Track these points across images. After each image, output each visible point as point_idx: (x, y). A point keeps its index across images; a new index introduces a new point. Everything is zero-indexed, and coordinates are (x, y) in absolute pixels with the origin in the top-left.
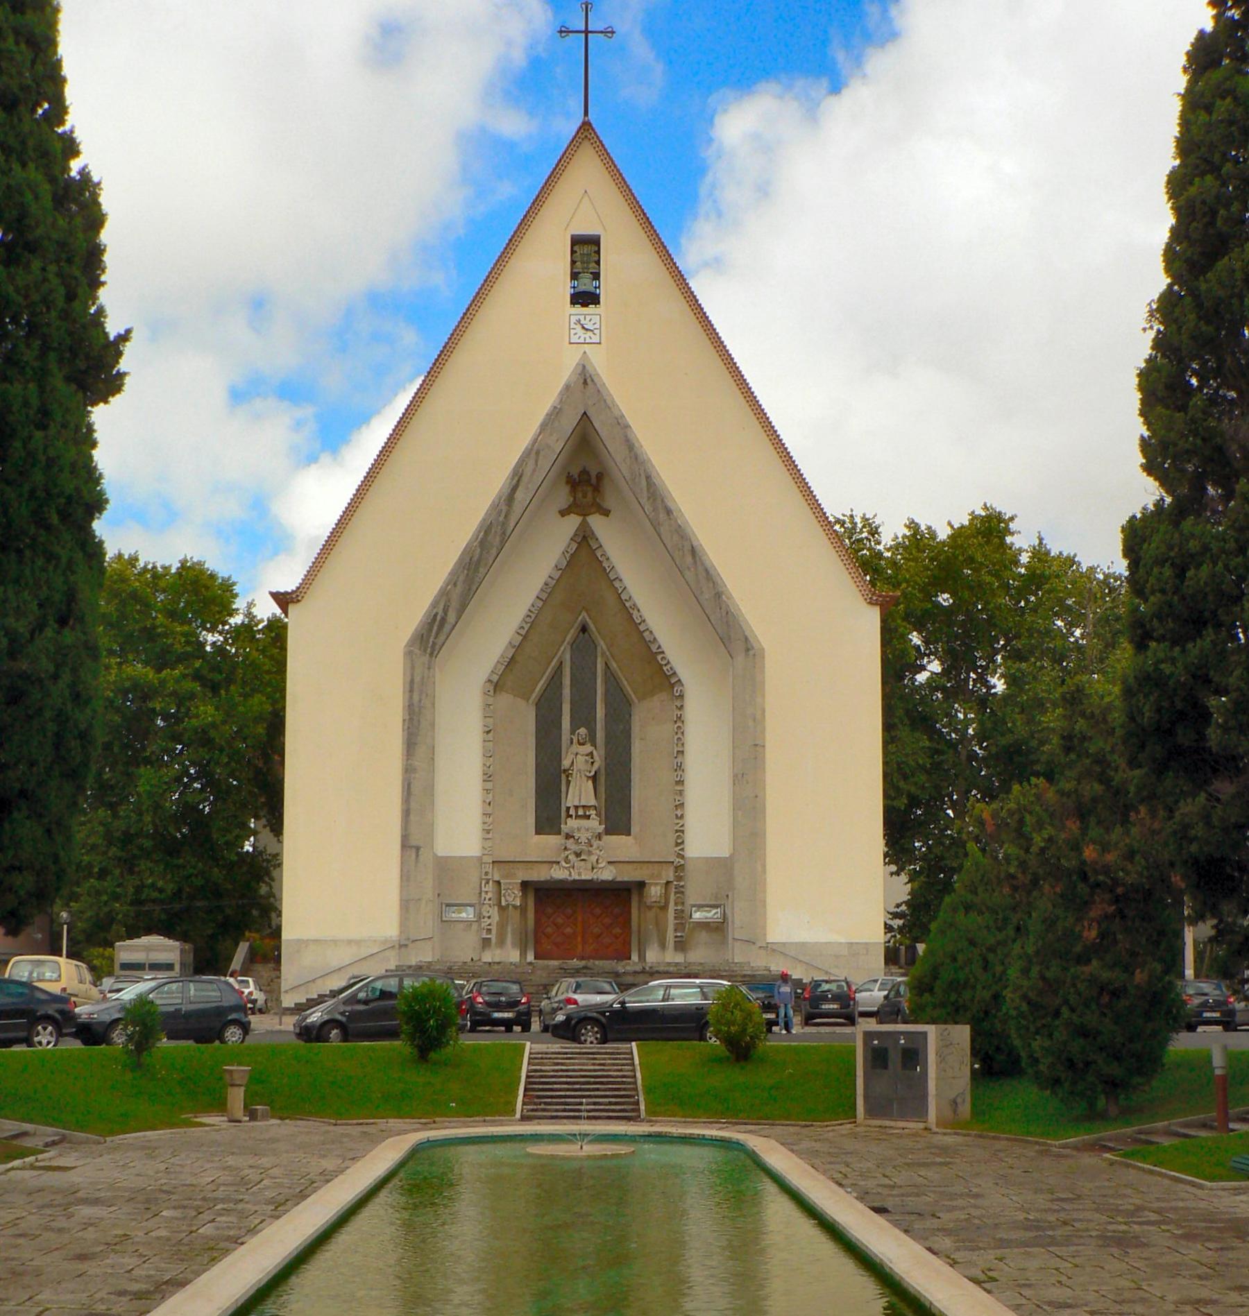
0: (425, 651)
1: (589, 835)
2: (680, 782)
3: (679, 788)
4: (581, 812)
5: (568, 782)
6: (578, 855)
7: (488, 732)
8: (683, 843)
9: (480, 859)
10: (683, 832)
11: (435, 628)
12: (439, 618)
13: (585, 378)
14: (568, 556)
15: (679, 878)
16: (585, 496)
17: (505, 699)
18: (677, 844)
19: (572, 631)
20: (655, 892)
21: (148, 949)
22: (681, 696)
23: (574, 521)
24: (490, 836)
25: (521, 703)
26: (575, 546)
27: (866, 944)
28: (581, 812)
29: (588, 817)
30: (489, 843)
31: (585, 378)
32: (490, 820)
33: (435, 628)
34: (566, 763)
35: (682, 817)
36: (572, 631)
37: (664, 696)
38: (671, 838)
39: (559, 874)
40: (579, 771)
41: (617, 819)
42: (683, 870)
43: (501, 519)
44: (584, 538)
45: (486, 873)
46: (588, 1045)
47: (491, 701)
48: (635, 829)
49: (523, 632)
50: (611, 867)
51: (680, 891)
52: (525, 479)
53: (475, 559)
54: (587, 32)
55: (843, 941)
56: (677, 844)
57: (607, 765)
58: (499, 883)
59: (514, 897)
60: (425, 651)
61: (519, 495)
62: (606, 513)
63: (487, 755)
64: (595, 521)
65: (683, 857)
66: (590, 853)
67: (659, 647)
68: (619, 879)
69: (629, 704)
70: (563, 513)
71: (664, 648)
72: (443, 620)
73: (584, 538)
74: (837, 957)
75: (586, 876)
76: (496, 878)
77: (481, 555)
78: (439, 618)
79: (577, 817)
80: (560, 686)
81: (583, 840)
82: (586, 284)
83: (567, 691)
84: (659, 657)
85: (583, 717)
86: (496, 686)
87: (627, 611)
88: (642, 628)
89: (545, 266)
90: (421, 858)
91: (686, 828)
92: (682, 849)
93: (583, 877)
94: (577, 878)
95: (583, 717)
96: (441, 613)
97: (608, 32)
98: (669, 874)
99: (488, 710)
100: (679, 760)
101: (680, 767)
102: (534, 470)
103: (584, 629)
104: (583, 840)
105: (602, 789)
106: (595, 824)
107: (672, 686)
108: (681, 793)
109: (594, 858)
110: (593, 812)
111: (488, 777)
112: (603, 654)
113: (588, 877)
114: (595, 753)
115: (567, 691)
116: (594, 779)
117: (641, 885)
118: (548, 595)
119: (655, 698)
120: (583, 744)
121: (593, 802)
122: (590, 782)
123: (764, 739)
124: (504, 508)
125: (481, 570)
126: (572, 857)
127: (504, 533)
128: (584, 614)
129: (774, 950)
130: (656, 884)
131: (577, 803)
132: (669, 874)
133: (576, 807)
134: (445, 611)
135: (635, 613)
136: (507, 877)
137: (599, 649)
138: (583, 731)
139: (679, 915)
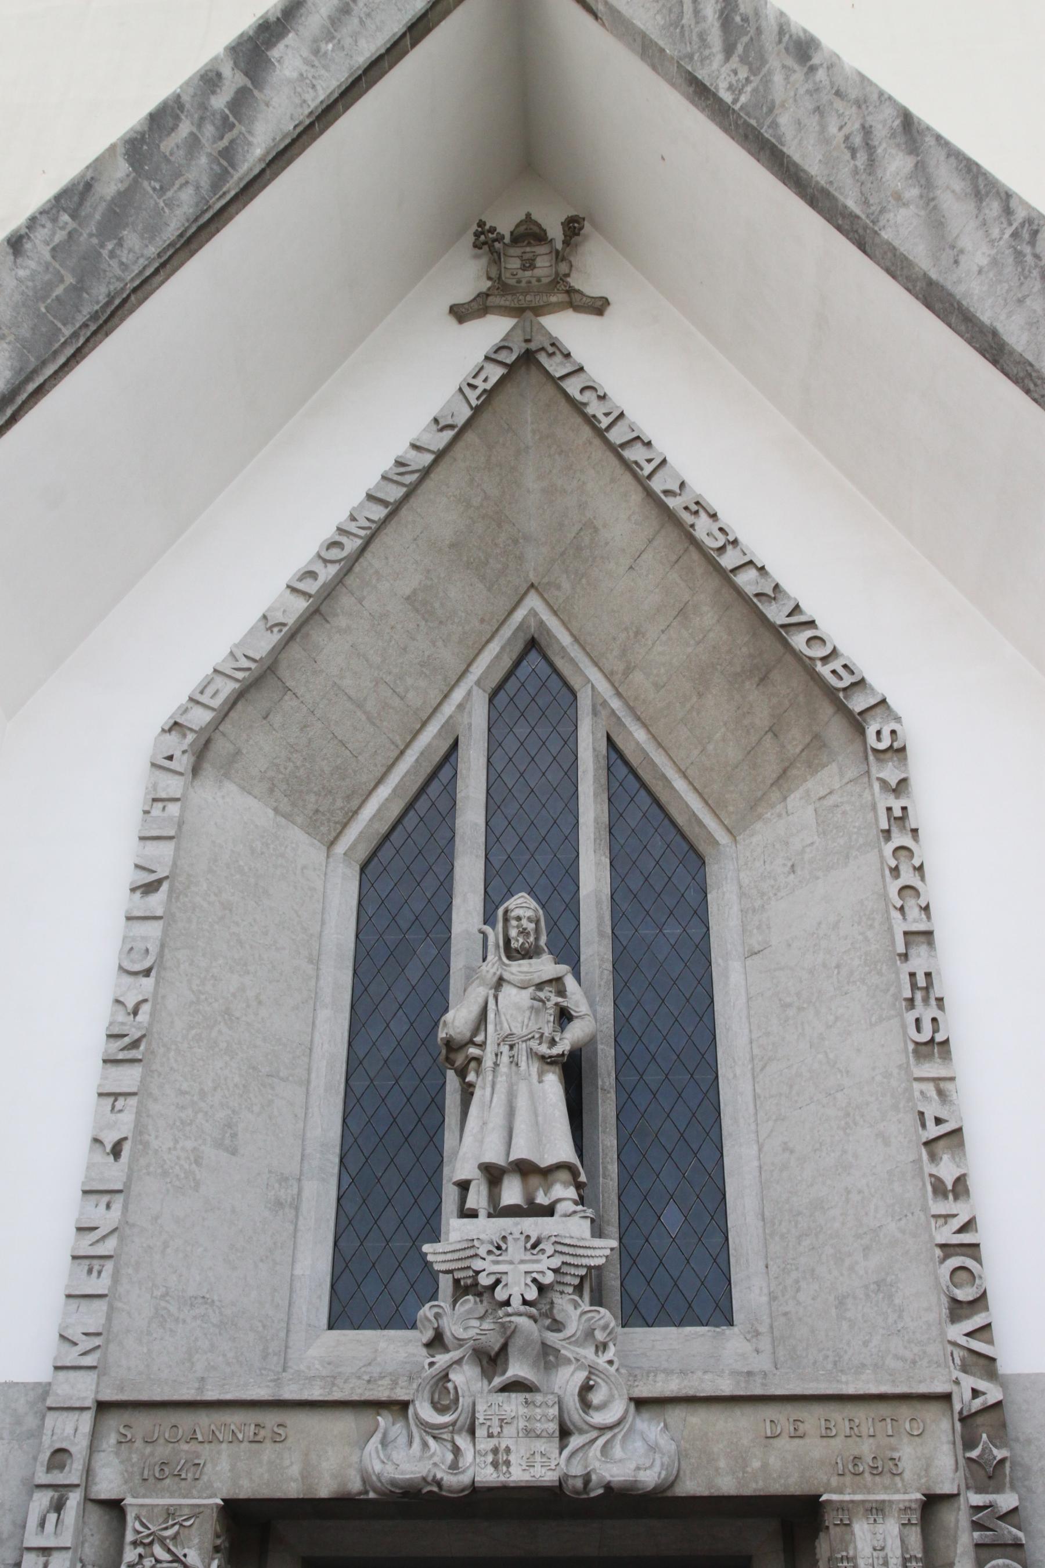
1: (544, 1266)
2: (935, 1048)
3: (932, 1069)
4: (512, 1193)
5: (467, 1092)
6: (491, 1360)
7: (150, 888)
8: (980, 1302)
9: (45, 1390)
10: (973, 1250)
14: (472, 395)
15: (988, 1475)
16: (529, 264)
18: (958, 1309)
19: (494, 648)
23: (494, 329)
24: (100, 1285)
25: (305, 849)
26: (495, 373)
28: (512, 1193)
29: (549, 1211)
30: (93, 1316)
32: (106, 1218)
34: (457, 1020)
35: (960, 1188)
36: (494, 648)
38: (922, 1290)
39: (401, 1458)
40: (510, 1041)
41: (672, 1259)
42: (1001, 1433)
43: (219, 102)
44: (526, 363)
45: (59, 1457)
47: (173, 786)
48: (749, 1291)
49: (312, 587)
50: (649, 1428)
53: (108, 189)
56: (958, 1309)
57: (621, 1022)
58: (115, 1507)
61: (289, 58)
62: (599, 307)
64: (564, 326)
66: (548, 1357)
67: (797, 609)
68: (691, 1486)
69: (692, 858)
70: (460, 313)
73: (526, 363)
75: (534, 1464)
76: (107, 1486)
79: (498, 1211)
80: (446, 813)
81: (517, 1287)
84: (799, 640)
85: (531, 855)
86: (202, 746)
88: (729, 560)
92: (984, 1331)
93: (518, 1475)
94: (487, 1476)
95: (531, 855)
98: (933, 1457)
99: (163, 823)
100: (919, 963)
101: (924, 988)
103: (533, 644)
104: (517, 1287)
105: (605, 1107)
106: (575, 1232)
107: (857, 724)
108: (942, 1087)
109: (567, 1381)
110: (563, 1191)
111: (126, 1048)
112: (599, 706)
113: (544, 1475)
114: (570, 982)
116: (573, 1070)
118: (410, 486)
119: (794, 800)
120: (527, 953)
121: (563, 1150)
122: (553, 1086)
124: (233, 80)
125: (132, 239)
126: (466, 1379)
127: (228, 155)
128: (533, 601)
130: (877, 1510)
131: (494, 1155)
132: (933, 1457)
133: (494, 1175)
135: (702, 527)
136: (160, 1474)
137: (585, 702)
138: (522, 906)
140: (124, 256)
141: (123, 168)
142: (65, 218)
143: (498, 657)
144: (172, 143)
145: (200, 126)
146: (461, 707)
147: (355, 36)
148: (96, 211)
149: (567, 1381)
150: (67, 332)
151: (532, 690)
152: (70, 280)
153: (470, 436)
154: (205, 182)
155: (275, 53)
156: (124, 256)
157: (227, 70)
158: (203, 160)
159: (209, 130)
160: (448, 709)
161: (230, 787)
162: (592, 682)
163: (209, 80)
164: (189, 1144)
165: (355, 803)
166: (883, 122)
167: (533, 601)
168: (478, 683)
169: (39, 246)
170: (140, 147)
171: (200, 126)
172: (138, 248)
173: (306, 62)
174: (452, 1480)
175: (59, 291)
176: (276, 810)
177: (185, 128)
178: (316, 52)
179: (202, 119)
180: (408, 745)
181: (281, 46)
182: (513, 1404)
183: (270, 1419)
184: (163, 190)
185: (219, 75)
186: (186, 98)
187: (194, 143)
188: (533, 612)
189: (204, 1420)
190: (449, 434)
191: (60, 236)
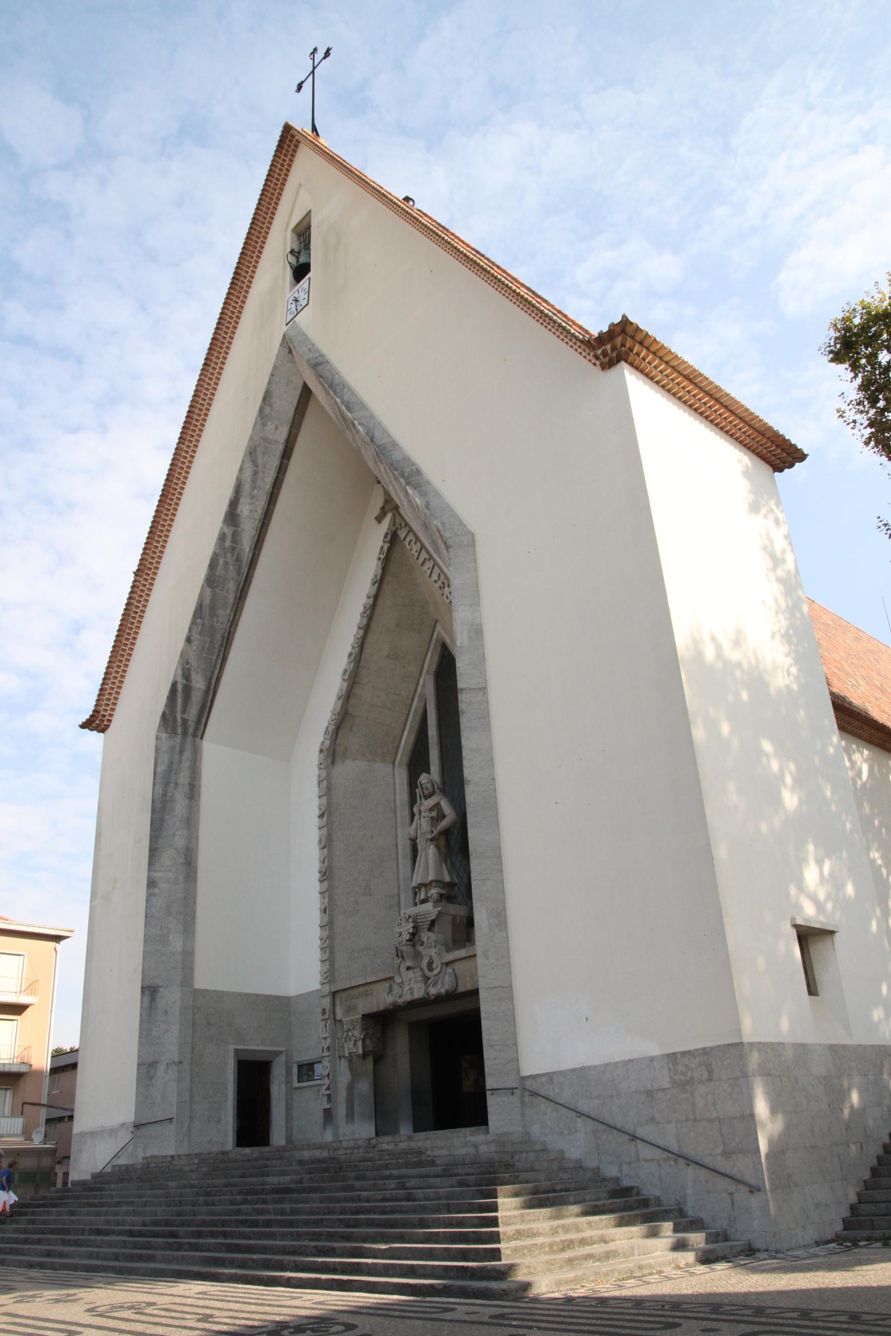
0: (174, 732)
11: (179, 701)
12: (180, 687)
19: (429, 654)
25: (382, 769)
27: (705, 1051)
33: (179, 701)
43: (228, 543)
46: (636, 1257)
52: (246, 488)
53: (207, 601)
55: (655, 1051)
60: (174, 732)
61: (244, 508)
63: (327, 843)
72: (187, 689)
74: (649, 1093)
77: (214, 594)
78: (180, 687)
86: (332, 754)
90: (161, 1004)
96: (180, 679)
99: (327, 788)
102: (256, 473)
111: (326, 874)
123: (483, 675)
125: (220, 612)
127: (238, 560)
129: (534, 1094)
134: (186, 675)
140: (221, 620)
141: (208, 590)
142: (199, 620)
143: (431, 658)
144: (219, 571)
145: (225, 557)
146: (423, 686)
147: (263, 480)
148: (206, 612)
150: (214, 657)
152: (208, 640)
153: (388, 578)
154: (235, 575)
155: (239, 510)
156: (221, 620)
157: (226, 530)
158: (231, 568)
159: (229, 555)
160: (419, 689)
161: (349, 762)
163: (222, 538)
164: (353, 899)
165: (397, 743)
167: (439, 627)
168: (427, 673)
169: (196, 636)
170: (211, 580)
171: (225, 557)
172: (224, 614)
173: (251, 504)
174: (400, 1001)
175: (207, 646)
176: (368, 761)
177: (221, 561)
178: (252, 497)
179: (225, 554)
180: (410, 710)
181: (240, 506)
182: (410, 973)
183: (368, 988)
184: (223, 588)
185: (224, 534)
186: (217, 551)
187: (226, 564)
188: (439, 633)
189: (355, 992)
190: (376, 585)
191: (200, 627)
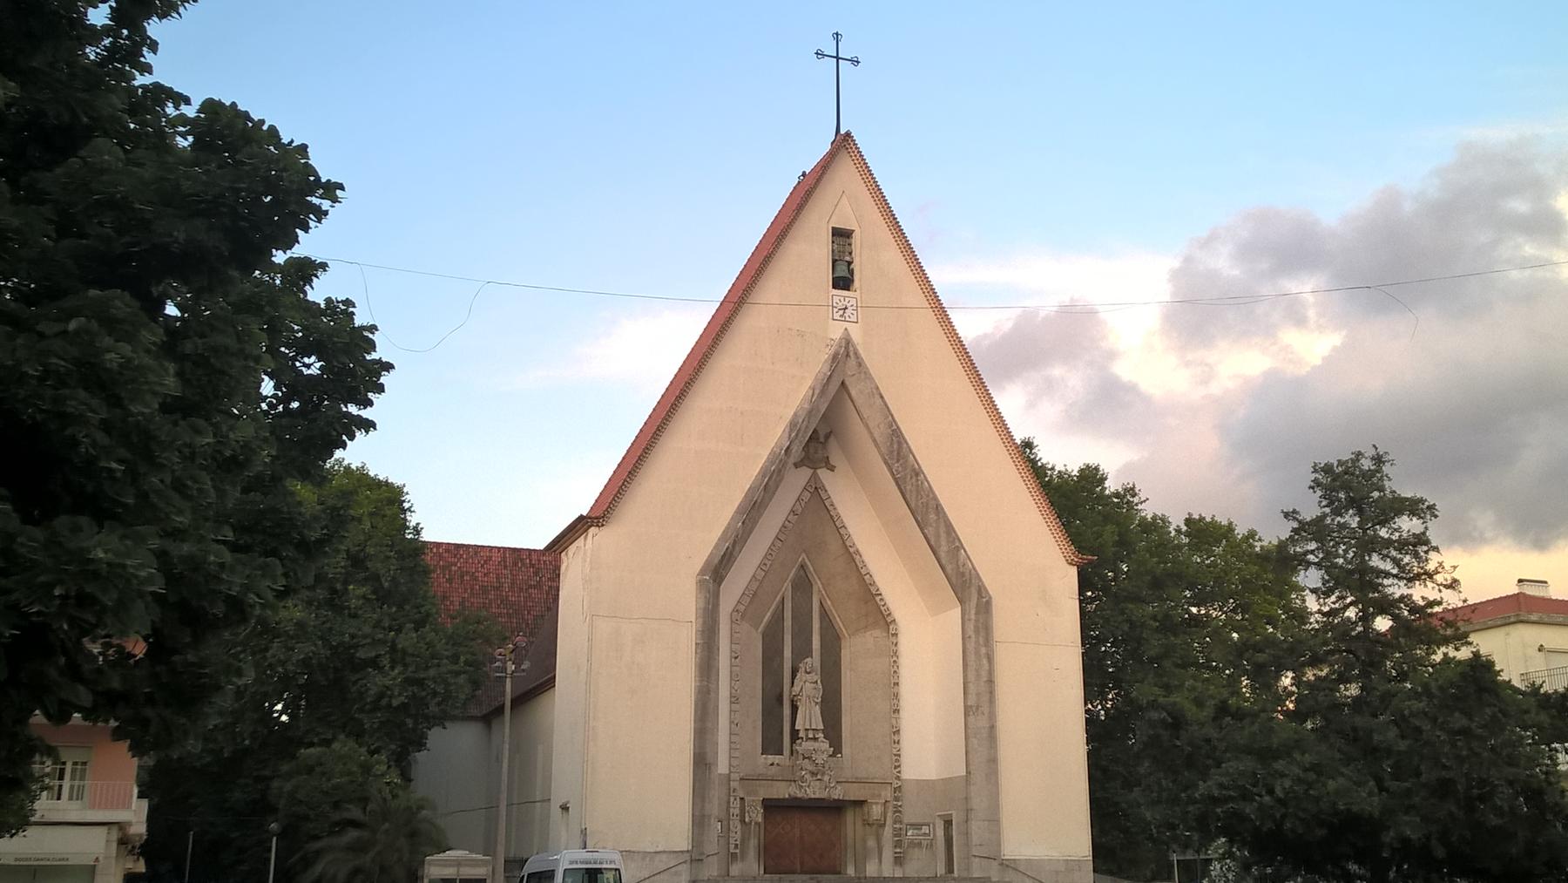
2: (897, 711)
6: (813, 774)
13: (845, 354)
15: (897, 799)
17: (745, 626)
20: (876, 811)
21: (458, 863)
22: (896, 635)
23: (805, 473)
31: (845, 354)
37: (877, 633)
51: (897, 810)
54: (838, 58)
59: (758, 815)
62: (832, 469)
65: (898, 778)
71: (882, 590)
74: (1057, 872)
75: (824, 795)
79: (808, 739)
82: (842, 271)
83: (788, 623)
87: (851, 557)
88: (863, 571)
89: (809, 253)
91: (903, 753)
97: (855, 62)
98: (887, 794)
101: (896, 696)
107: (888, 625)
110: (821, 735)
115: (788, 623)
117: (860, 804)
136: (748, 794)
137: (815, 589)
139: (897, 833)
149: (826, 778)
151: (803, 585)
162: (818, 585)
166: (932, 503)
